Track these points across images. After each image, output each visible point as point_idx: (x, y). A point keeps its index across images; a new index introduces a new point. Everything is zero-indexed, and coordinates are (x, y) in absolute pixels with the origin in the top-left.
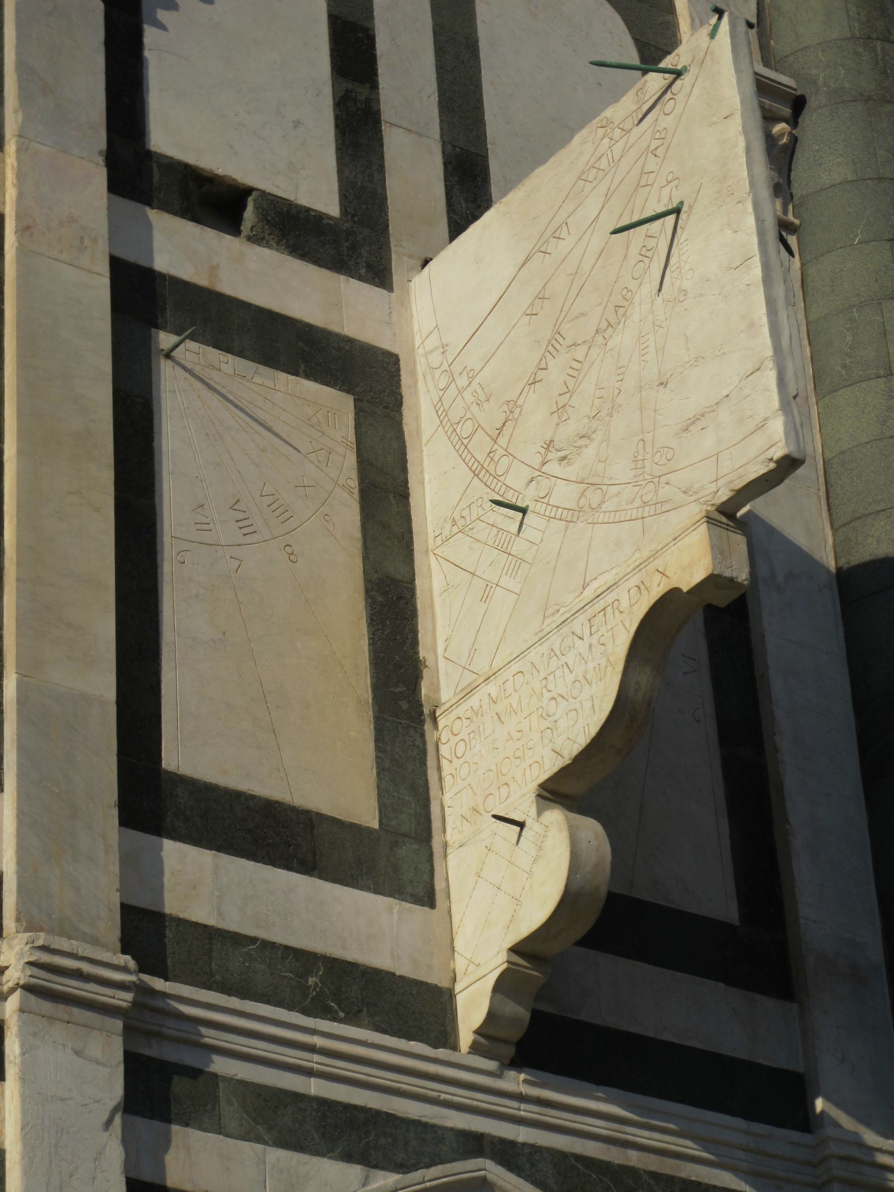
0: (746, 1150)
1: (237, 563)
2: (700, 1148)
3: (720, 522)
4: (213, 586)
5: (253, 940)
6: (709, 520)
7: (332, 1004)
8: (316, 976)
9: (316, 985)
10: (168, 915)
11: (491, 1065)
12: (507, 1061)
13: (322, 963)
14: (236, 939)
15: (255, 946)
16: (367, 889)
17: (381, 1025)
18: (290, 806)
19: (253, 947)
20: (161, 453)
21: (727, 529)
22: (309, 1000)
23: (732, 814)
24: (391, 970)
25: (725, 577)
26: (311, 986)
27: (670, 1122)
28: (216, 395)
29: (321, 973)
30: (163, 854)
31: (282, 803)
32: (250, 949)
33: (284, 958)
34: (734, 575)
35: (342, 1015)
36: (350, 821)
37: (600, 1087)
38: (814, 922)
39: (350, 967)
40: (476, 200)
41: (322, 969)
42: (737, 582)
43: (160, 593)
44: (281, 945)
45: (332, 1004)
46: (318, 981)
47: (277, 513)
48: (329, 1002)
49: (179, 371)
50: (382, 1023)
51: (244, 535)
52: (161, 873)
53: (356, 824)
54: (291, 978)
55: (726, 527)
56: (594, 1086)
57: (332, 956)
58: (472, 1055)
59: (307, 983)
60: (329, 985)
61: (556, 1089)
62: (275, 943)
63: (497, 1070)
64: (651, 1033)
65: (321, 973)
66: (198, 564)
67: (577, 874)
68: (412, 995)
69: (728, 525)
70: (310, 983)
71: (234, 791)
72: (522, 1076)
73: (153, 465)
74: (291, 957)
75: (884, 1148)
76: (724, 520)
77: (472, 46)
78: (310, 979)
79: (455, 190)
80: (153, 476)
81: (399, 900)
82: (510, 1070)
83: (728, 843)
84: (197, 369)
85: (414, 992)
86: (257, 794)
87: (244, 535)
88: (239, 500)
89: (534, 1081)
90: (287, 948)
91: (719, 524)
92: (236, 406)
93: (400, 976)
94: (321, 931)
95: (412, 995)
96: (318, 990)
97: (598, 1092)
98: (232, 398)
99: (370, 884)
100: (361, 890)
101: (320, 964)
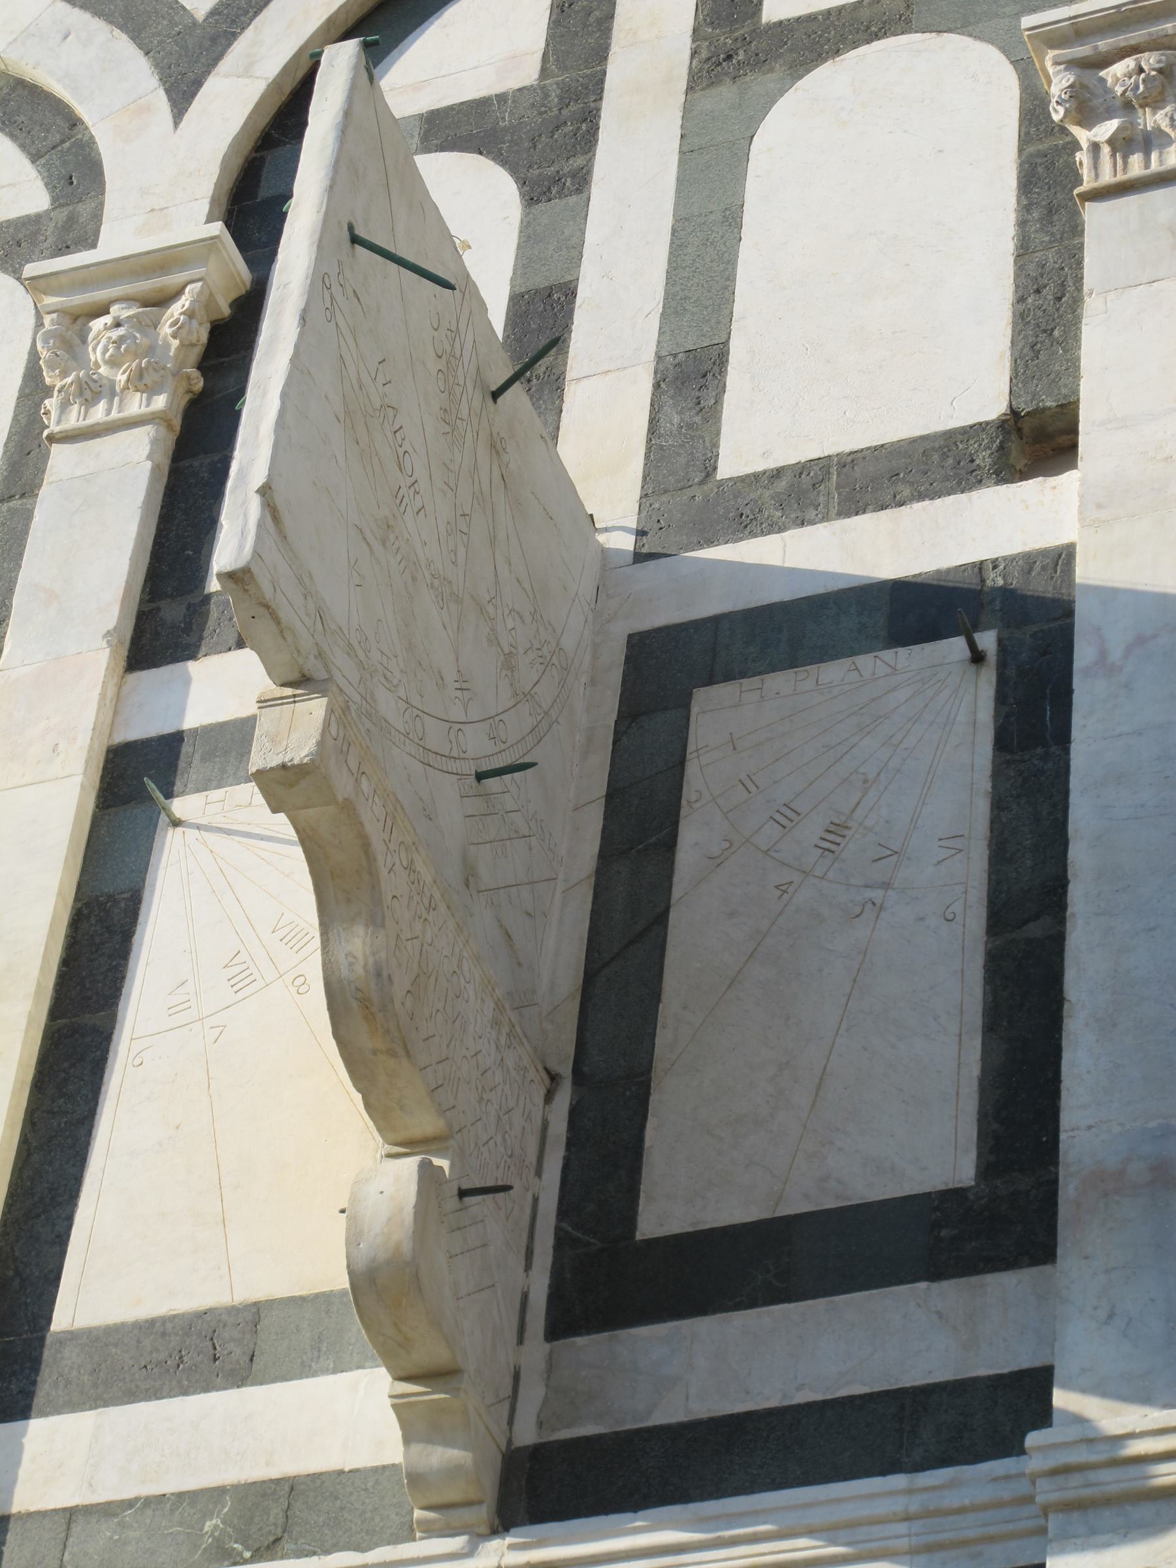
0: (908, 1518)
1: (217, 1031)
2: (821, 1543)
3: (282, 698)
4: (176, 1074)
5: (129, 1504)
6: (261, 705)
7: (236, 1546)
8: (218, 1516)
9: (216, 1527)
10: (14, 1515)
11: (457, 1543)
12: (484, 1529)
13: (231, 1497)
14: (107, 1510)
15: (133, 1510)
16: (326, 1371)
17: (307, 1547)
18: (226, 1308)
19: (130, 1512)
20: (141, 945)
21: (295, 702)
22: (200, 1552)
23: (990, 1028)
24: (338, 1467)
25: (272, 769)
26: (207, 1533)
27: (764, 1523)
28: (236, 838)
29: (226, 1510)
30: (24, 1440)
31: (216, 1309)
32: (125, 1516)
33: (172, 1511)
34: (286, 760)
35: (247, 1555)
36: (316, 1291)
37: (641, 1514)
38: (1090, 1128)
39: (273, 1487)
40: (699, 403)
41: (229, 1503)
42: (293, 766)
43: (97, 1117)
44: (173, 1494)
45: (236, 1546)
46: (219, 1522)
47: (290, 944)
48: (232, 1544)
49: (192, 833)
50: (309, 1545)
51: (236, 992)
52: (17, 1463)
53: (323, 1294)
54: (179, 1533)
55: (292, 700)
56: (629, 1515)
57: (249, 1481)
58: (424, 1541)
59: (202, 1530)
60: (236, 1522)
61: (541, 1543)
62: (165, 1495)
63: (463, 1548)
64: (774, 1403)
65: (226, 1510)
66: (160, 1058)
67: (359, 1244)
68: (366, 1490)
69: (295, 696)
70: (206, 1529)
71: (147, 1321)
72: (509, 1540)
73: (126, 965)
74: (185, 1504)
75: (1137, 1431)
76: (289, 691)
77: (733, 219)
78: (208, 1523)
79: (665, 408)
80: (124, 977)
81: (371, 1367)
82: (489, 1540)
83: (975, 1070)
84: (218, 821)
85: (370, 1485)
86: (181, 1312)
87: (236, 992)
88: (239, 952)
89: (523, 1543)
90: (180, 1495)
91: (280, 702)
92: (262, 838)
93: (350, 1471)
94: (238, 1454)
95: (366, 1490)
96: (216, 1534)
97: (634, 1521)
98: (257, 831)
99: (328, 1365)
100: (313, 1376)
101: (228, 1498)
